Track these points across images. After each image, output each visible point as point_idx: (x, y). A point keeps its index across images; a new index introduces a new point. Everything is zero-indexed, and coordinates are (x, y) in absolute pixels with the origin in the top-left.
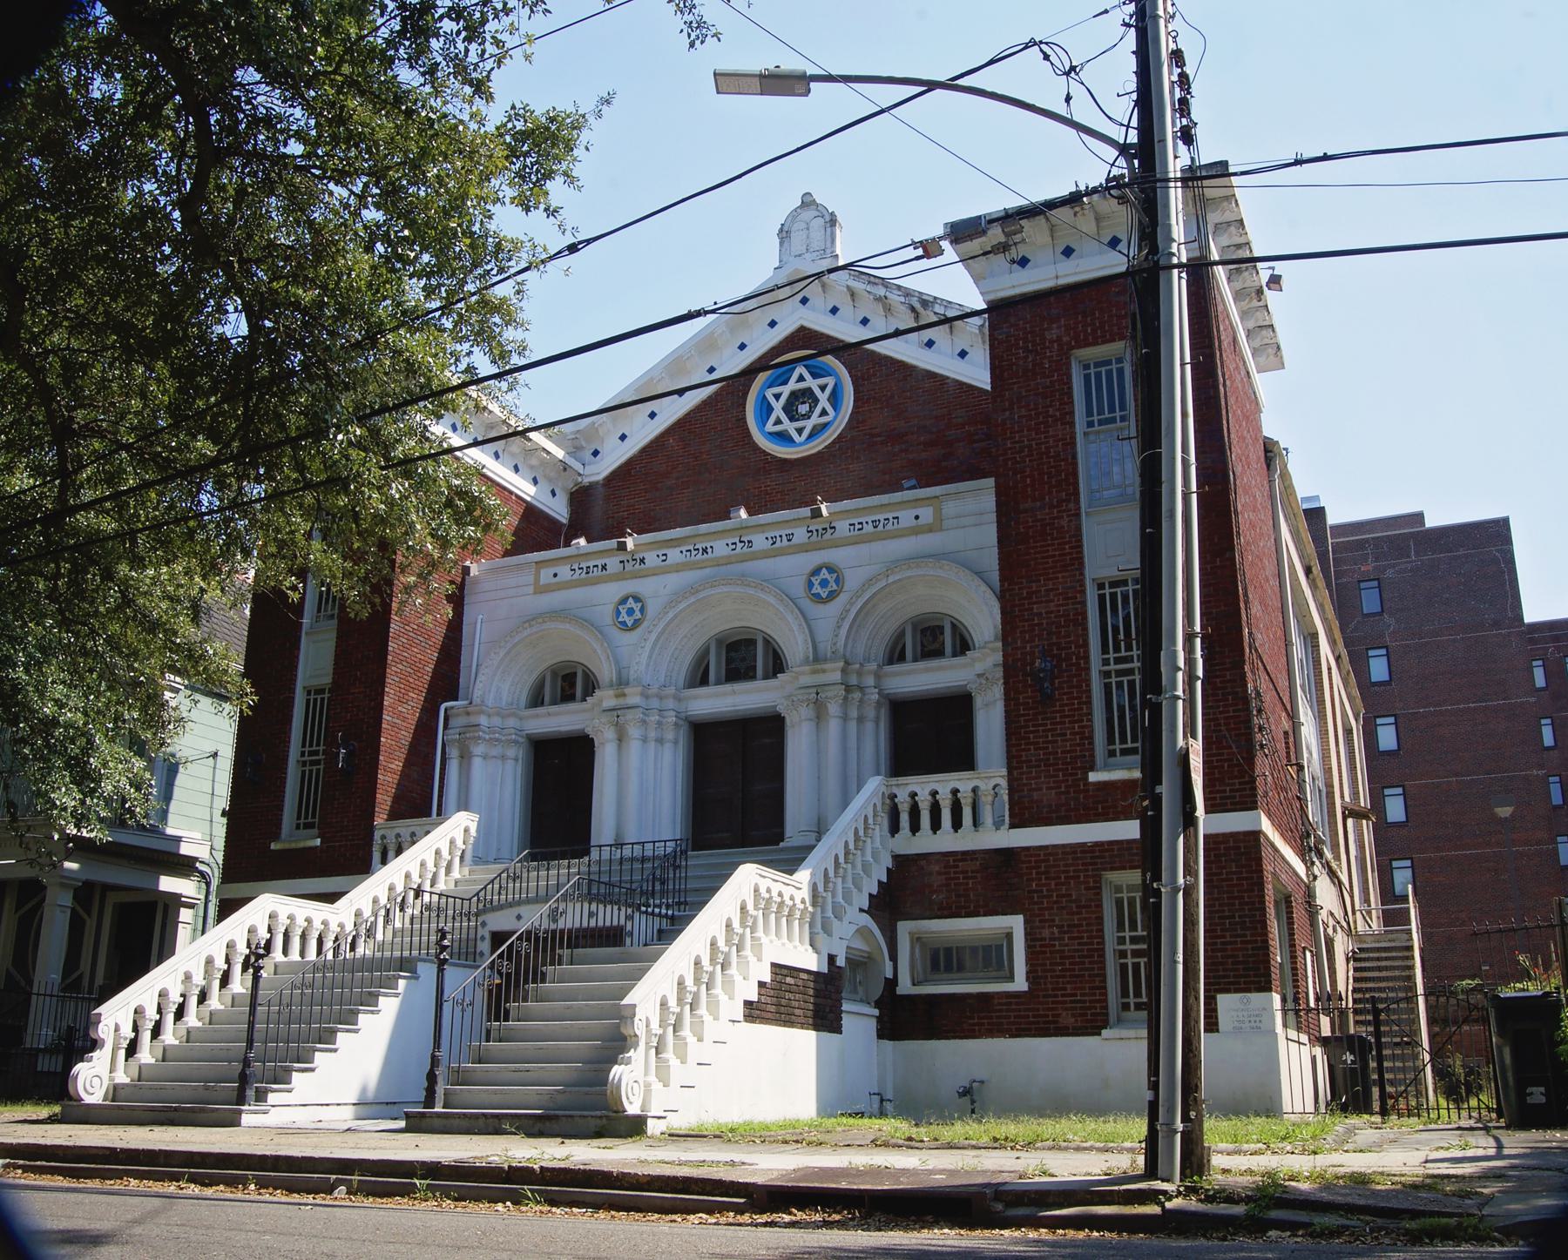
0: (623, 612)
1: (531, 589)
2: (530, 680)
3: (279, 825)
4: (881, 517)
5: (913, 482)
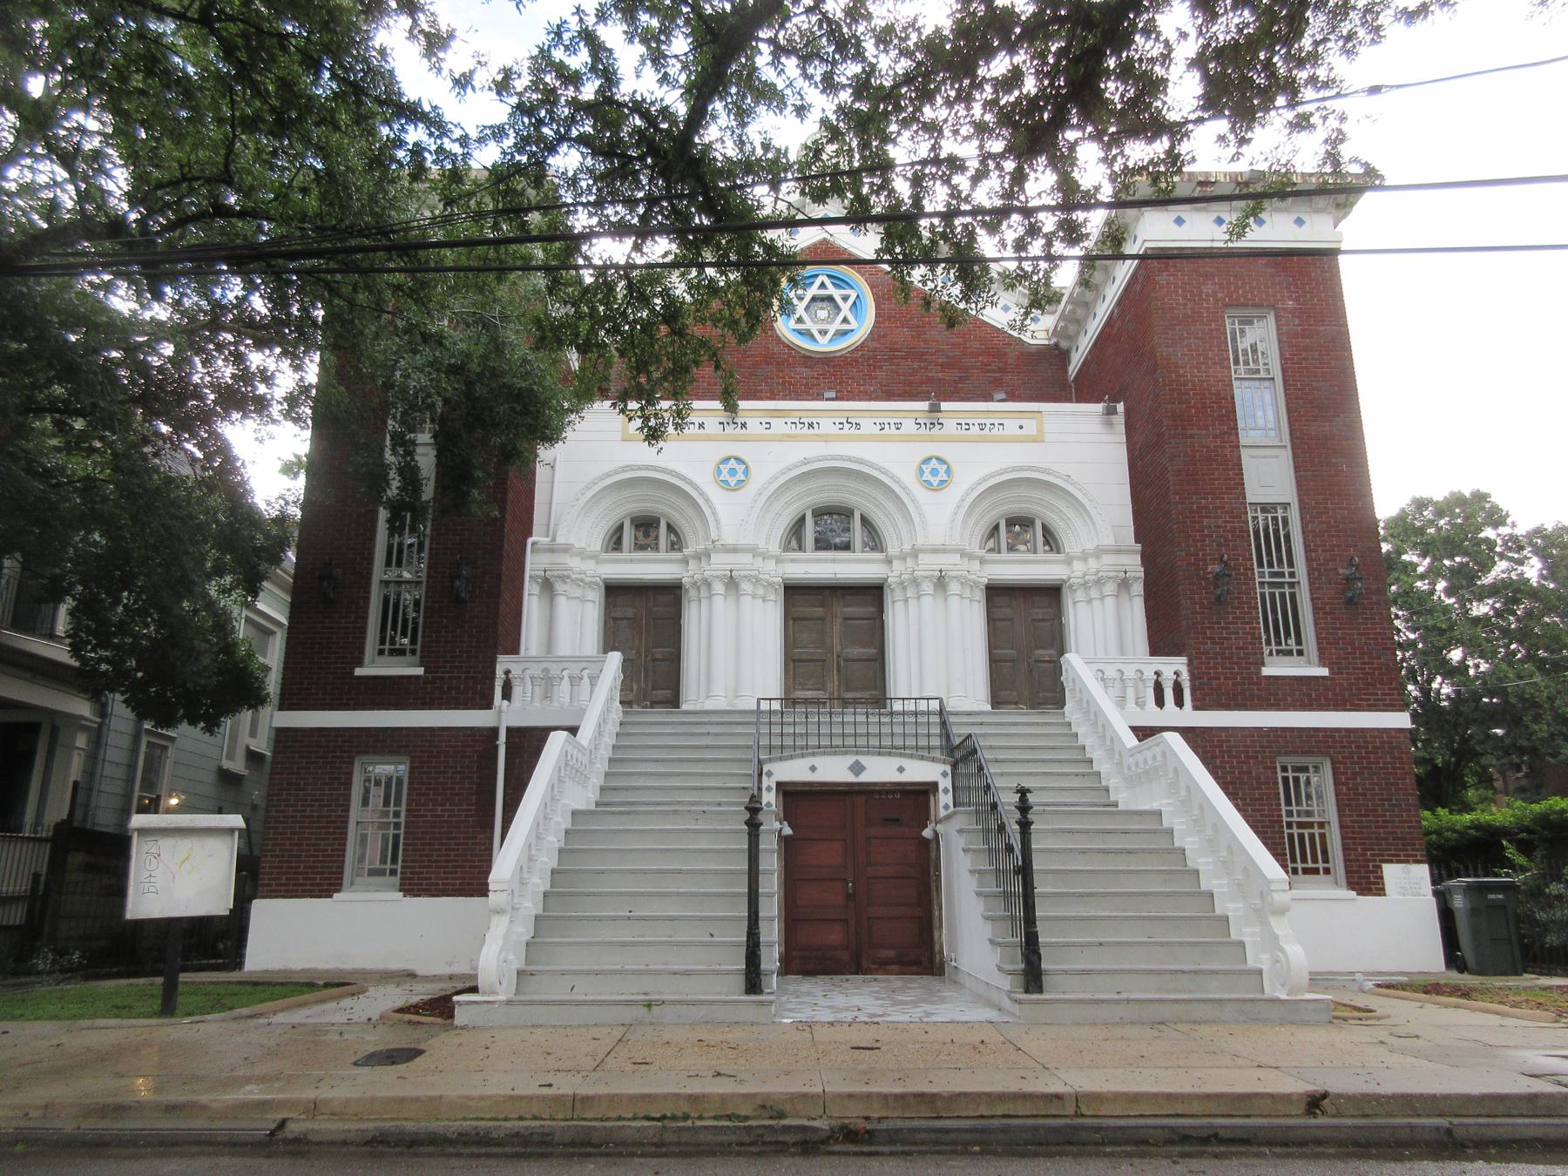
0: (725, 472)
1: (618, 436)
2: (607, 524)
3: (362, 652)
4: (988, 422)
5: (833, 394)
